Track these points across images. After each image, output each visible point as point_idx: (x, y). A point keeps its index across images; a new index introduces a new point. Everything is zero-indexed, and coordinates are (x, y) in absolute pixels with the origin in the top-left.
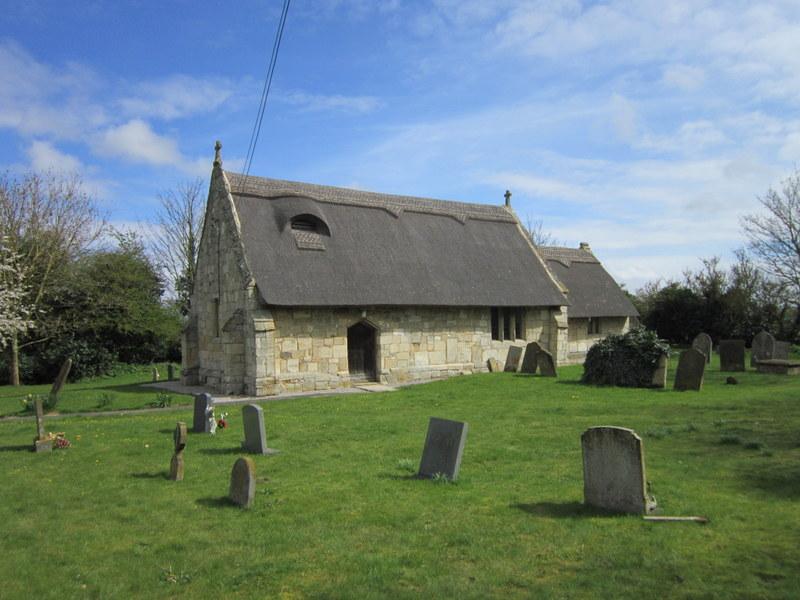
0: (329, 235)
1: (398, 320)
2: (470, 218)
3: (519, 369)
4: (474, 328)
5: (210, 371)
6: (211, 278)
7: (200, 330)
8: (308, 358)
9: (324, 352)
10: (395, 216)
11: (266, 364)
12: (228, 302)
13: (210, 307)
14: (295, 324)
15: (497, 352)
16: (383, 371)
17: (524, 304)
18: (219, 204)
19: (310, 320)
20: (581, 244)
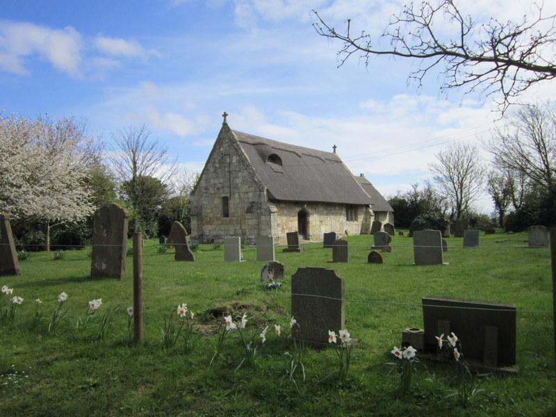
0: (281, 165)
1: (315, 209)
4: (341, 214)
6: (219, 185)
7: (204, 214)
8: (285, 227)
10: (300, 156)
12: (240, 198)
13: (218, 202)
16: (311, 234)
17: (358, 203)
19: (285, 208)
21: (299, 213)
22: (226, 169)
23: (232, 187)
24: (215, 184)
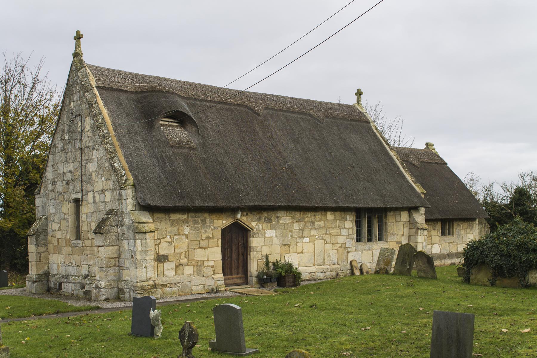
1: (269, 221)
2: (327, 117)
5: (66, 276)
6: (69, 176)
7: (50, 233)
8: (184, 261)
9: (199, 255)
12: (94, 202)
13: (68, 208)
14: (172, 225)
18: (81, 98)
19: (186, 222)
20: (427, 144)
21: (223, 231)
22: (78, 145)
23: (85, 179)
24: (64, 174)
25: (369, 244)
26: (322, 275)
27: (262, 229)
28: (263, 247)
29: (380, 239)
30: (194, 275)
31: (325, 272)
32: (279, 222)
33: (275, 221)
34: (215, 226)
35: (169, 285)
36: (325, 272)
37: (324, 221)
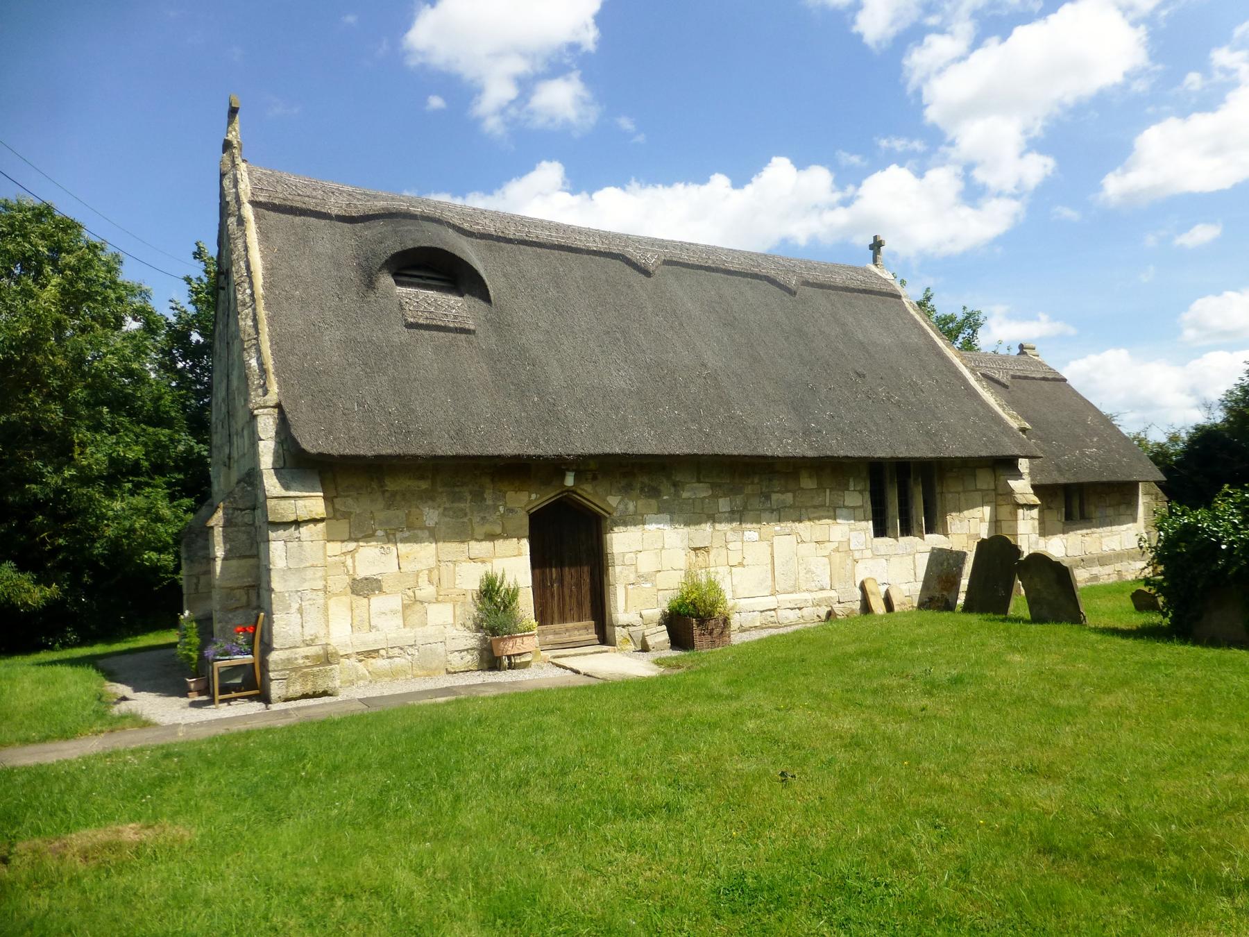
0: (484, 295)
1: (654, 493)
3: (962, 598)
8: (427, 591)
10: (646, 273)
11: (300, 611)
15: (897, 567)
19: (428, 497)
25: (905, 540)
26: (792, 616)
27: (635, 513)
28: (639, 555)
29: (930, 529)
30: (454, 624)
31: (800, 609)
32: (679, 496)
33: (669, 495)
34: (509, 505)
35: (383, 652)
36: (800, 609)
37: (794, 492)
